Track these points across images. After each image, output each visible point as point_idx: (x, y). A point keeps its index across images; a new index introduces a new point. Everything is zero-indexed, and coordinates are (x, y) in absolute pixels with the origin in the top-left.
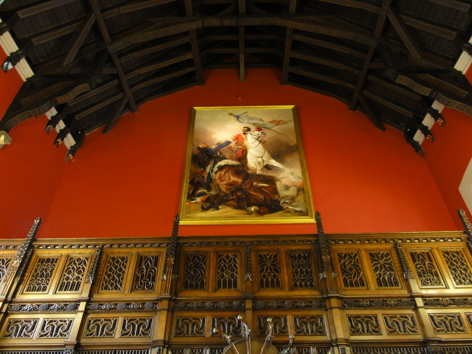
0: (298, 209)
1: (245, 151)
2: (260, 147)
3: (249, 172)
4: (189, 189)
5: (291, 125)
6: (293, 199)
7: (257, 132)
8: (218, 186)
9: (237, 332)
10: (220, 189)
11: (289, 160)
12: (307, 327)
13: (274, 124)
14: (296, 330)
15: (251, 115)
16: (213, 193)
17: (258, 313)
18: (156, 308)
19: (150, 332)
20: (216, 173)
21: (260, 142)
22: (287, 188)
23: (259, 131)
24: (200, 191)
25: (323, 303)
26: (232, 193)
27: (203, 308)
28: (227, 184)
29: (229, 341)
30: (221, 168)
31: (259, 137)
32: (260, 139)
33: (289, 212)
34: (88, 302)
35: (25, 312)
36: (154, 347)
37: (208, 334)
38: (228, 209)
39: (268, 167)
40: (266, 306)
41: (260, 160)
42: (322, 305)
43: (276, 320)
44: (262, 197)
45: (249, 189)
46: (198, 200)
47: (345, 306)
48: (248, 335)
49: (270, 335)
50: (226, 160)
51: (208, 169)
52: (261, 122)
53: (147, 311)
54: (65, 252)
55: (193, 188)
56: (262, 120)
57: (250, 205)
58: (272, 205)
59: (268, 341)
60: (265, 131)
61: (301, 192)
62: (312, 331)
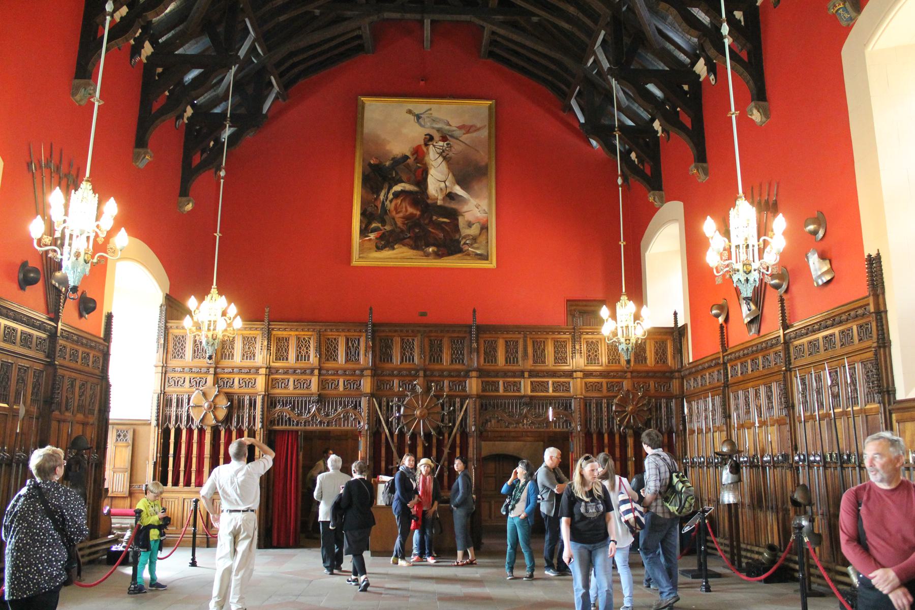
0: (478, 252)
1: (425, 172)
2: (444, 167)
3: (429, 201)
4: (361, 222)
5: (484, 133)
6: (474, 239)
7: (441, 143)
8: (394, 219)
9: (413, 389)
10: (396, 224)
11: (476, 187)
13: (463, 131)
15: (435, 115)
16: (388, 228)
20: (391, 201)
21: (445, 158)
22: (470, 225)
23: (444, 141)
24: (374, 225)
26: (410, 229)
28: (404, 218)
30: (397, 195)
31: (443, 151)
32: (444, 154)
33: (469, 255)
34: (320, 370)
35: (280, 374)
38: (405, 249)
39: (451, 196)
41: (443, 185)
44: (441, 235)
45: (428, 224)
46: (372, 236)
50: (403, 184)
51: (382, 197)
52: (448, 127)
54: (293, 333)
55: (365, 221)
56: (448, 124)
57: (428, 246)
58: (450, 245)
60: (452, 141)
61: (484, 231)
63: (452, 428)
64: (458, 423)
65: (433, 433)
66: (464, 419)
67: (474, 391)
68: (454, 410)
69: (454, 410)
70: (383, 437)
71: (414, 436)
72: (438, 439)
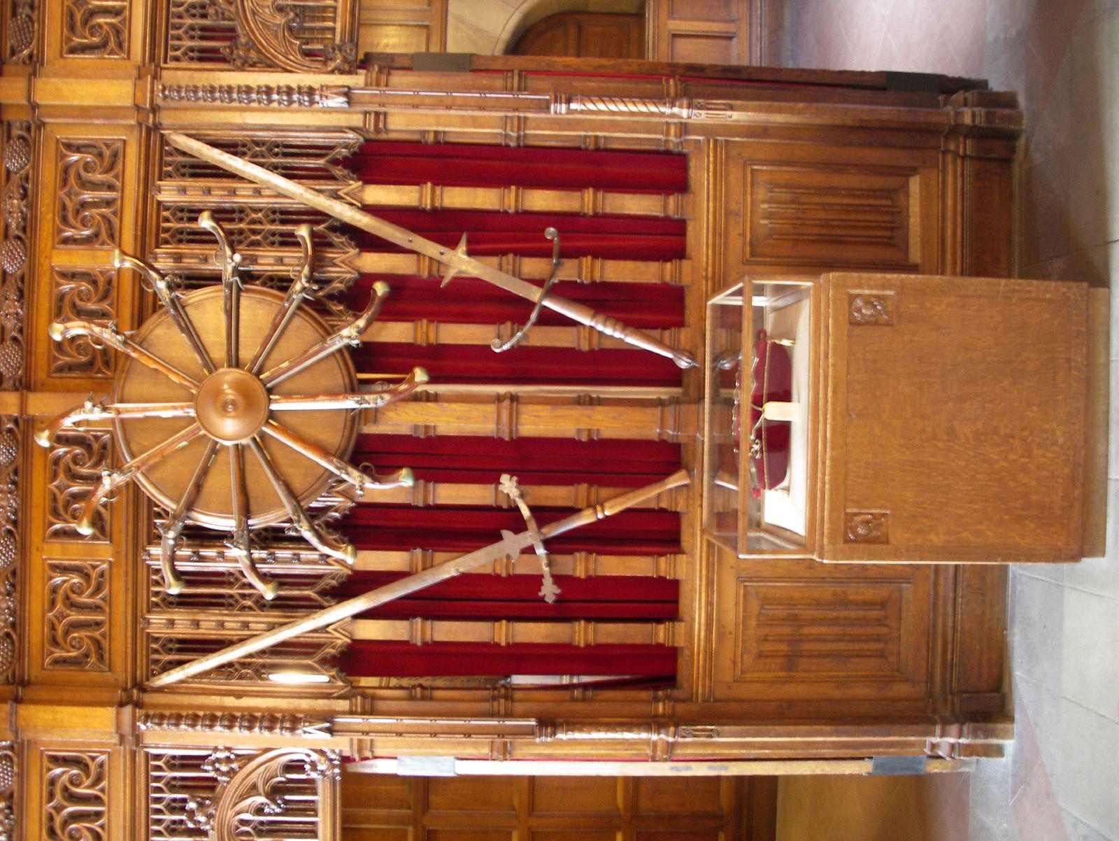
9: (101, 451)
12: (95, 205)
14: (103, 243)
17: (41, 374)
18: (11, 748)
19: (93, 758)
25: (16, 132)
27: (14, 573)
29: (119, 479)
36: (138, 738)
37: (103, 554)
40: (15, 339)
42: (21, 137)
43: (67, 309)
47: (31, 56)
48: (105, 409)
49: (107, 335)
53: (21, 776)
59: (125, 343)
62: (111, 188)
63: (331, 233)
64: (300, 194)
65: (349, 334)
66: (286, 156)
67: (118, 92)
68: (220, 215)
69: (220, 215)
70: (373, 630)
71: (373, 454)
72: (391, 311)
